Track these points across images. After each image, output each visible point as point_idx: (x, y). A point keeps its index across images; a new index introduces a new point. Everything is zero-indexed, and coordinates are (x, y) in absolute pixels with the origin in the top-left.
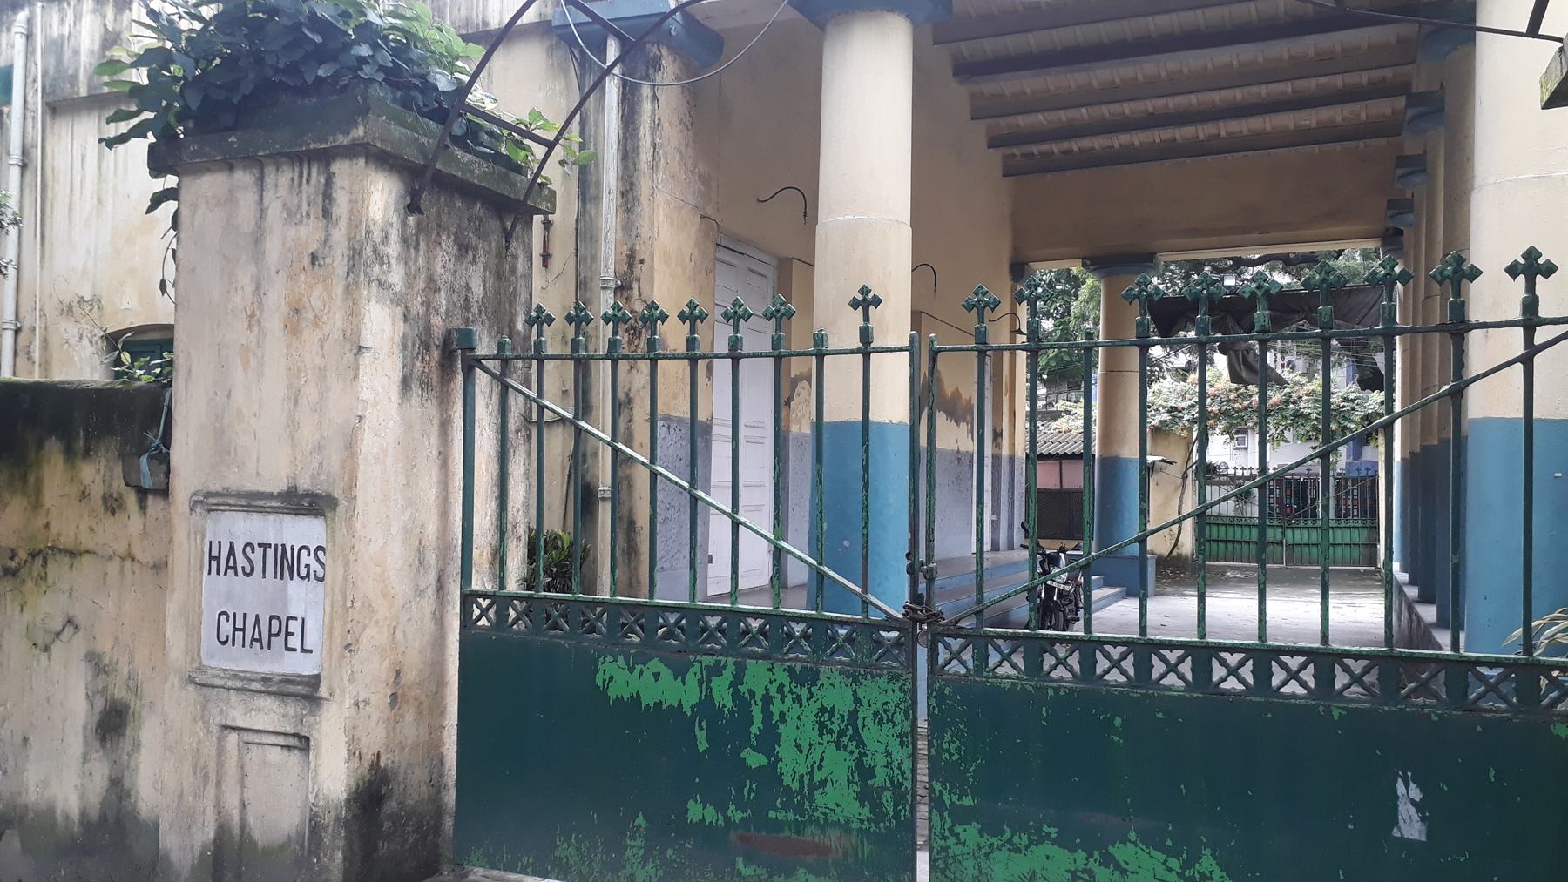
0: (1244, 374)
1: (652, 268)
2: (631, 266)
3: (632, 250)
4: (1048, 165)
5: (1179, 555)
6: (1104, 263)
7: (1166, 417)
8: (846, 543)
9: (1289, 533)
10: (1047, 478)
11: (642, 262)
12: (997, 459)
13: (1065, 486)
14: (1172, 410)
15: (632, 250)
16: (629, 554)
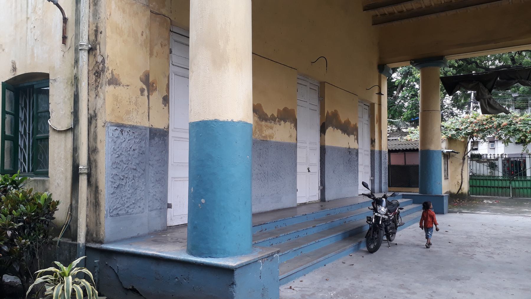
0: (488, 110)
1: (105, 37)
2: (96, 36)
3: (97, 27)
4: (391, 18)
5: (462, 193)
6: (421, 62)
7: (454, 132)
8: (203, 201)
9: (513, 183)
10: (398, 160)
11: (101, 33)
12: (372, 152)
13: (407, 164)
14: (457, 130)
15: (97, 27)
16: (96, 206)
